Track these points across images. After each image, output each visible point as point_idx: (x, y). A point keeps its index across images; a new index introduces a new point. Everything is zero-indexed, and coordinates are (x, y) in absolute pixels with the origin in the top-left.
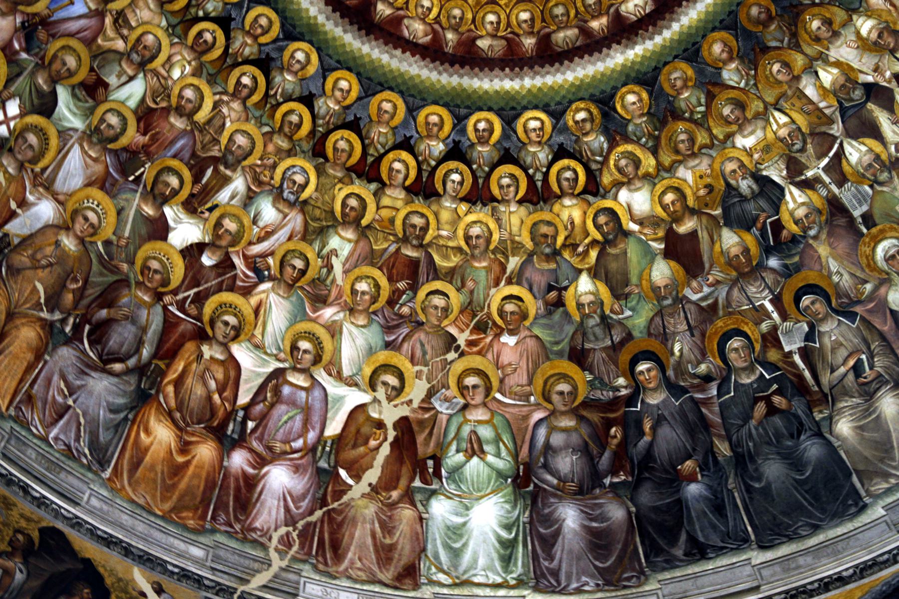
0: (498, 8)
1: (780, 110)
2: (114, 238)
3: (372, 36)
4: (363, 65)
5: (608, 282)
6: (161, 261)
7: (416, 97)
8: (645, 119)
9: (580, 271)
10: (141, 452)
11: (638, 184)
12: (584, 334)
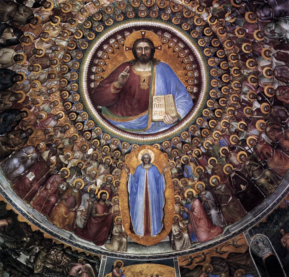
4: (208, 81)
6: (264, 108)
9: (225, 21)
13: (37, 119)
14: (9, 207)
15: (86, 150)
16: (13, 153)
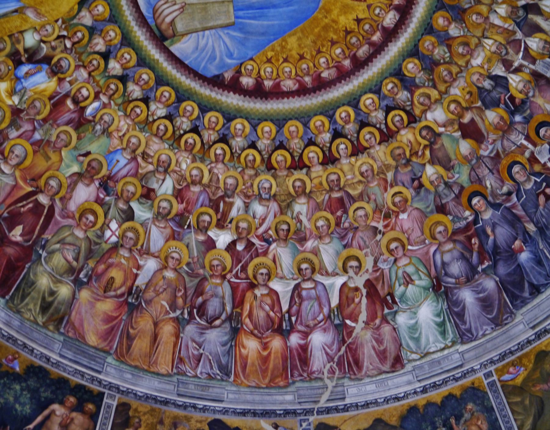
0: (323, 54)
1: (487, 38)
2: (190, 260)
3: (269, 99)
4: (272, 115)
5: (440, 164)
6: (218, 259)
7: (304, 118)
8: (422, 73)
9: (424, 165)
10: (244, 360)
11: (434, 107)
12: (440, 196)
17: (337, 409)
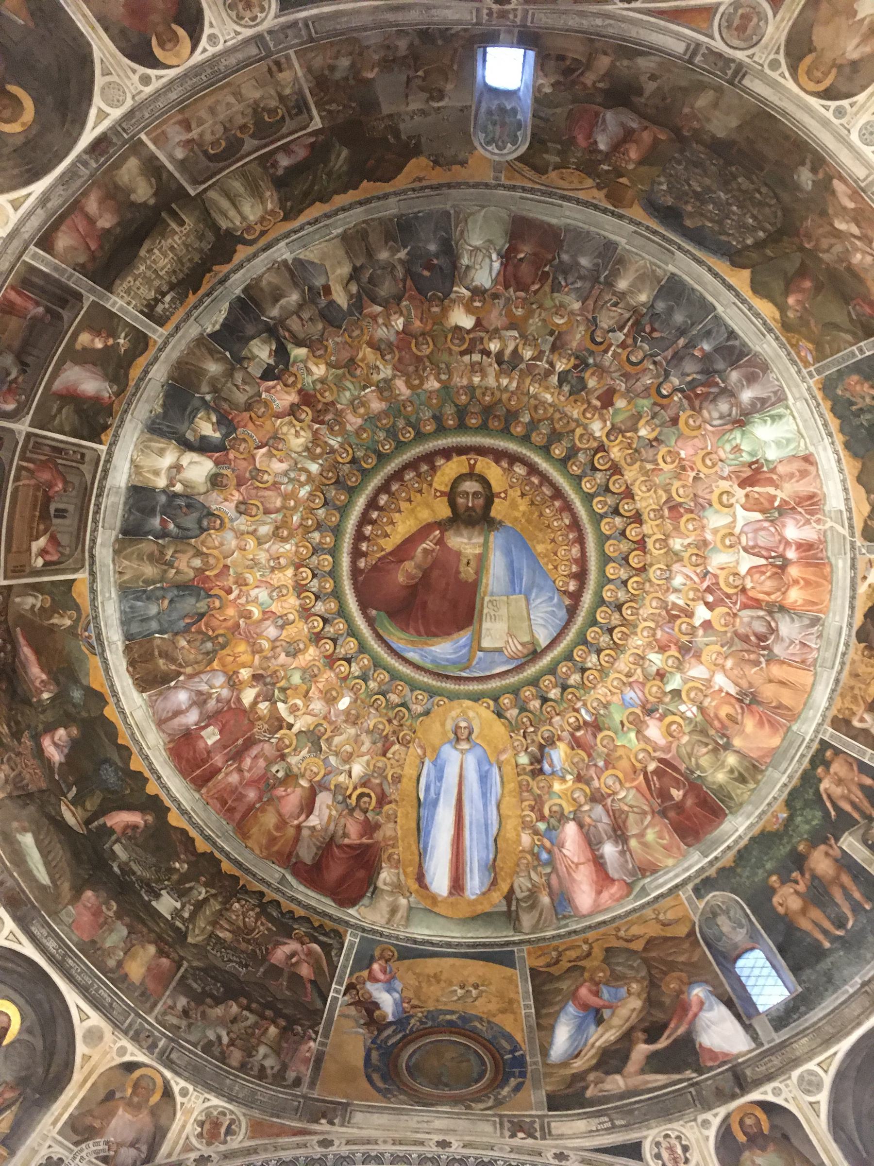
7: (603, 539)
13: (241, 617)
14: (152, 788)
15: (335, 698)
16: (182, 678)
17: (850, 519)
